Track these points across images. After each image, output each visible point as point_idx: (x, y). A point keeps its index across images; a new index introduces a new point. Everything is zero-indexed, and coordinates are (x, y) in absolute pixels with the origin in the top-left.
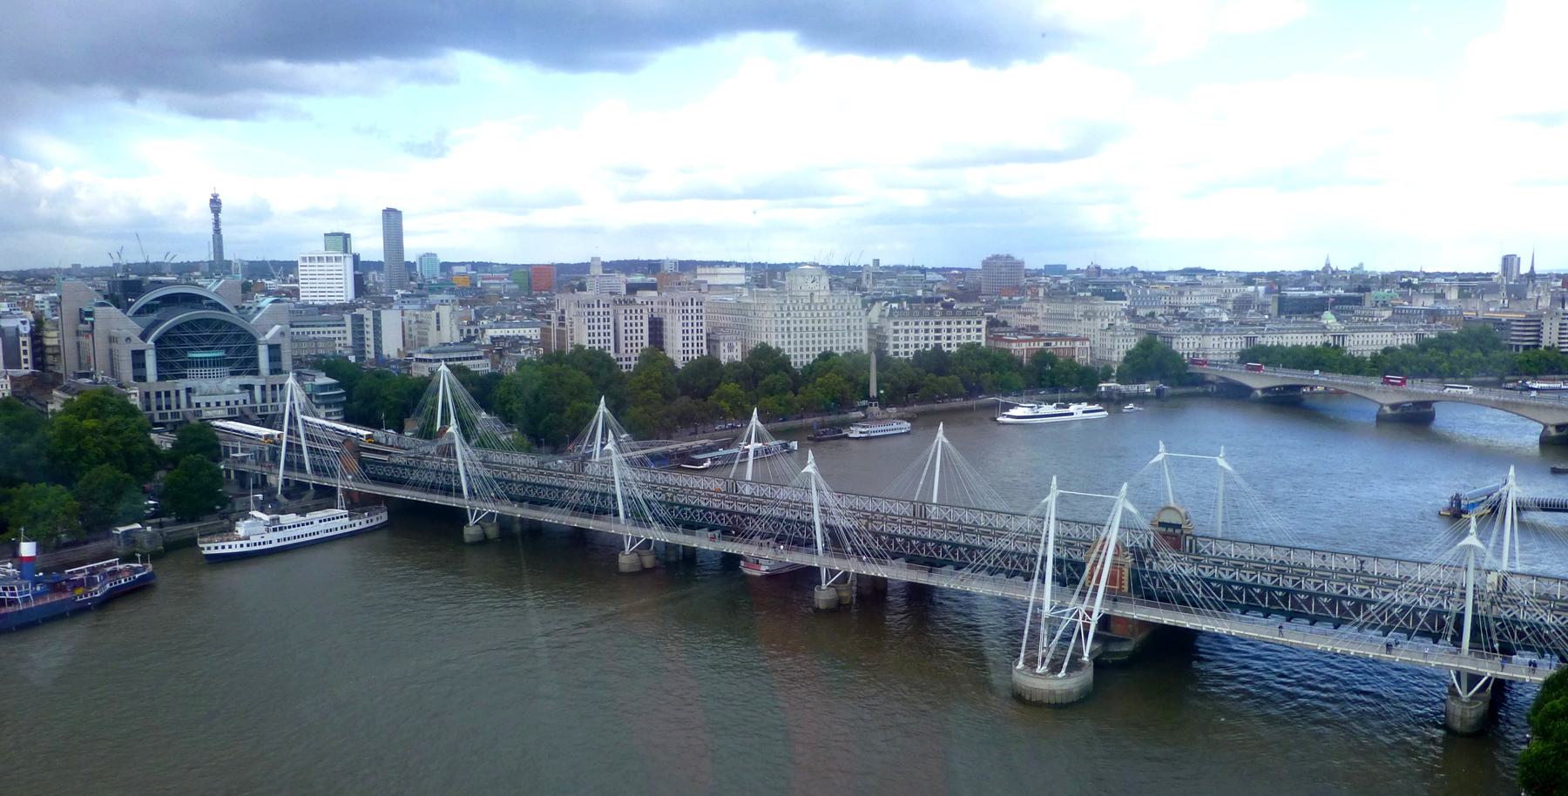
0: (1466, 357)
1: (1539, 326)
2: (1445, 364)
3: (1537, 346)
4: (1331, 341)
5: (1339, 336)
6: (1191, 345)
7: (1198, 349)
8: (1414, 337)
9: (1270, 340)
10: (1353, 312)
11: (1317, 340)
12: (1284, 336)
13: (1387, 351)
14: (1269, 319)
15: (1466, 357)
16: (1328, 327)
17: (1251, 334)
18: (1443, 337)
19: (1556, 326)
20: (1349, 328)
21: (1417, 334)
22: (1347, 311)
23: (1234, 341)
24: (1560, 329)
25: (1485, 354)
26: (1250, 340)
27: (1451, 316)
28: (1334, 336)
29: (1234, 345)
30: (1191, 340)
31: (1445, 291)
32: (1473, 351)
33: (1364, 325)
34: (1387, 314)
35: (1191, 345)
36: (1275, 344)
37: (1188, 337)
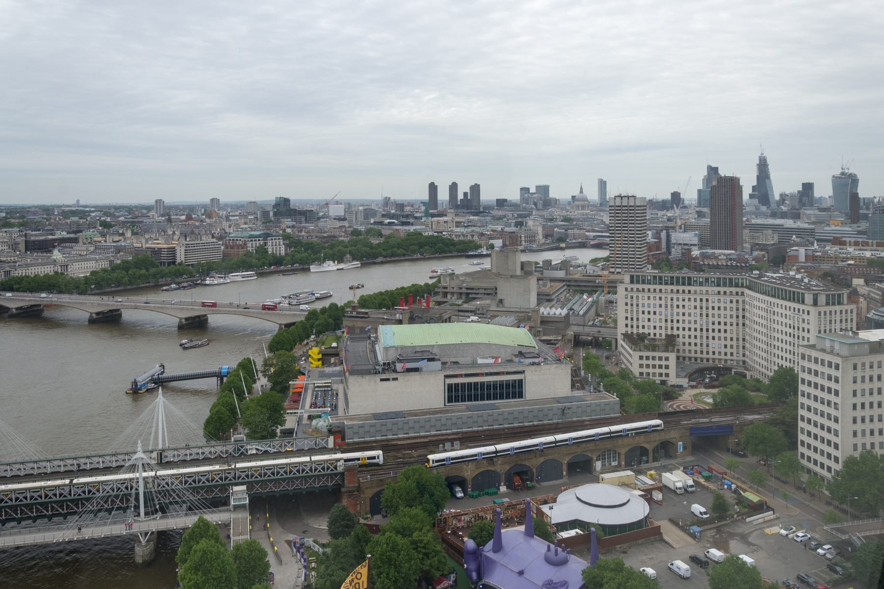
0: (137, 273)
1: (174, 251)
2: (126, 279)
3: (174, 263)
4: (59, 271)
5: (64, 266)
8: (108, 262)
9: (20, 272)
10: (72, 248)
11: (48, 270)
12: (30, 268)
13: (93, 273)
14: (20, 254)
15: (137, 273)
17: (8, 269)
18: (125, 262)
22: (70, 248)
25: (147, 270)
26: (7, 273)
28: (61, 266)
31: (125, 232)
32: (141, 269)
33: (79, 258)
34: (92, 249)
36: (24, 274)
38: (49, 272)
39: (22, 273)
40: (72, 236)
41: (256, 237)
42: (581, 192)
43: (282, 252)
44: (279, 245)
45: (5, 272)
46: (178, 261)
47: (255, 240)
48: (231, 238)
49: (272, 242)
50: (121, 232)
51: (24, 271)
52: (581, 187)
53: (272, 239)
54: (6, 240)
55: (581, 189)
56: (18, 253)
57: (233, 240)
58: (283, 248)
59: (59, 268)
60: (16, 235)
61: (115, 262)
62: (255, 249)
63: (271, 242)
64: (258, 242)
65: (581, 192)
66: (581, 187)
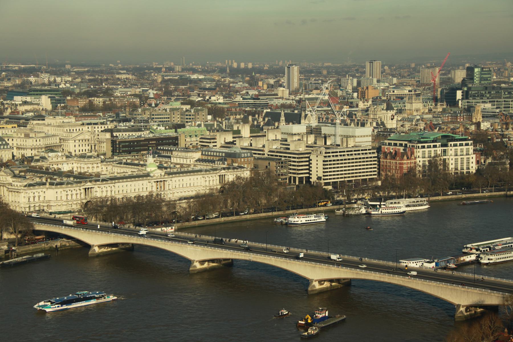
5: (161, 181)
6: (37, 199)
7: (43, 202)
8: (218, 178)
9: (104, 189)
19: (321, 163)
20: (169, 174)
21: (220, 176)
23: (74, 192)
24: (324, 165)
27: (244, 157)
28: (158, 182)
29: (74, 197)
30: (37, 194)
31: (240, 129)
35: (37, 199)
37: (34, 191)
38: (141, 190)
39: (107, 191)
40: (171, 133)
43: (471, 165)
44: (468, 154)
45: (85, 189)
46: (314, 179)
47: (429, 147)
48: (393, 142)
49: (456, 151)
50: (235, 128)
51: (109, 189)
53: (455, 145)
54: (87, 137)
56: (102, 157)
57: (395, 145)
58: (473, 158)
59: (154, 184)
60: (100, 130)
61: (226, 177)
62: (429, 161)
63: (453, 148)
64: (433, 150)
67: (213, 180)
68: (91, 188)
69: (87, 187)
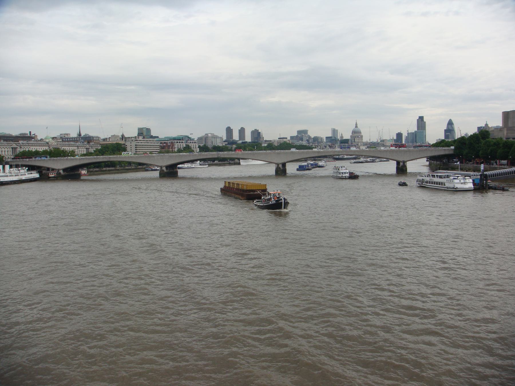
16: (50, 143)
41: (180, 140)
42: (356, 127)
45: (12, 148)
47: (180, 142)
52: (356, 123)
55: (356, 124)
65: (356, 127)
66: (356, 123)
67: (84, 151)
68: (16, 148)
69: (14, 147)
